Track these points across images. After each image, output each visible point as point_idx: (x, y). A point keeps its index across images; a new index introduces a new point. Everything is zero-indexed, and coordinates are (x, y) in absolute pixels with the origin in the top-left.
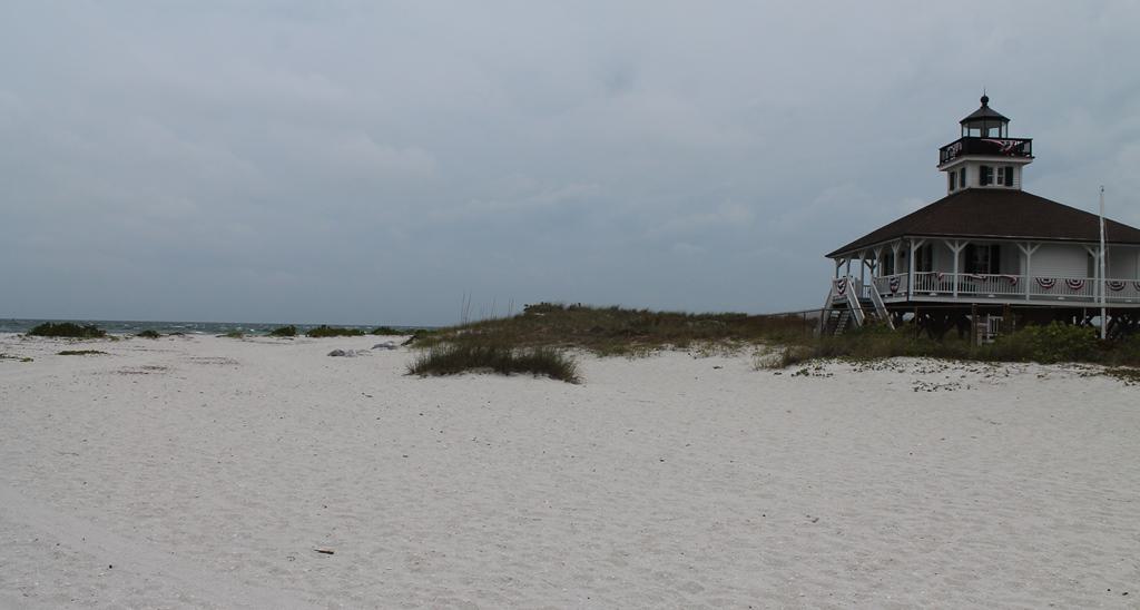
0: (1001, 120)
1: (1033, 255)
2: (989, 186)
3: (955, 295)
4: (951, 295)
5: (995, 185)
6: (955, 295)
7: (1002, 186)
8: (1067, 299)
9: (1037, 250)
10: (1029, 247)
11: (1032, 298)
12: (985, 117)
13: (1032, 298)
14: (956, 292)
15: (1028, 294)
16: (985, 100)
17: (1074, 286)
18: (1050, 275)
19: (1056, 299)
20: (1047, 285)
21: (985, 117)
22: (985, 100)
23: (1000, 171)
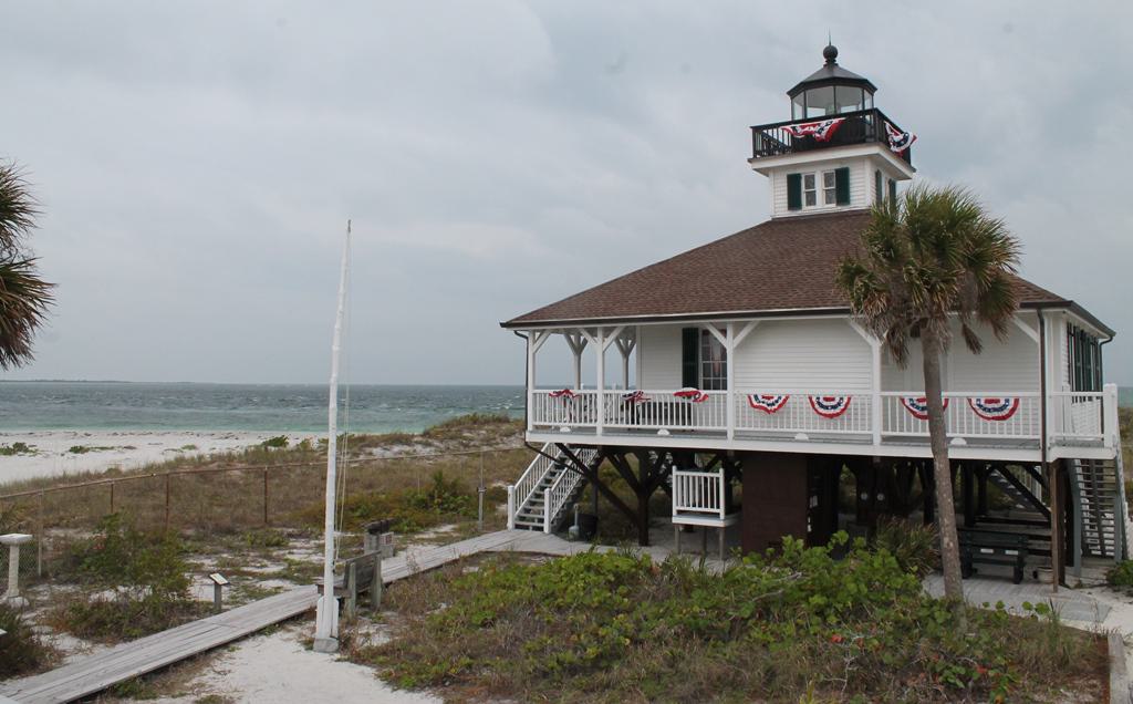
0: (865, 85)
1: (740, 347)
2: (806, 210)
3: (599, 431)
4: (593, 430)
5: (822, 206)
6: (599, 431)
7: (833, 207)
8: (813, 439)
9: (753, 331)
10: (730, 332)
11: (739, 436)
12: (832, 79)
13: (739, 436)
14: (600, 425)
15: (730, 428)
16: (831, 54)
17: (830, 408)
18: (777, 391)
19: (790, 438)
20: (771, 406)
21: (832, 79)
22: (831, 54)
23: (827, 178)
